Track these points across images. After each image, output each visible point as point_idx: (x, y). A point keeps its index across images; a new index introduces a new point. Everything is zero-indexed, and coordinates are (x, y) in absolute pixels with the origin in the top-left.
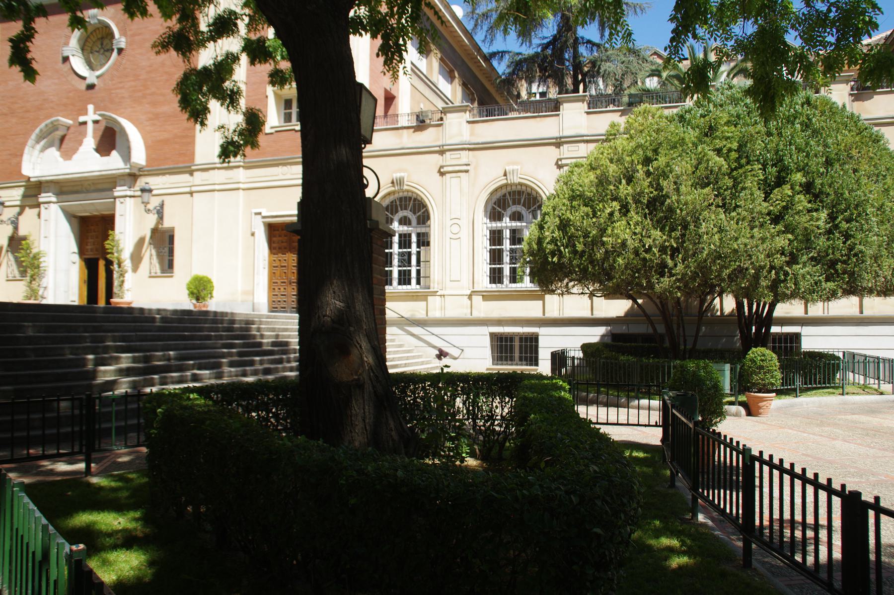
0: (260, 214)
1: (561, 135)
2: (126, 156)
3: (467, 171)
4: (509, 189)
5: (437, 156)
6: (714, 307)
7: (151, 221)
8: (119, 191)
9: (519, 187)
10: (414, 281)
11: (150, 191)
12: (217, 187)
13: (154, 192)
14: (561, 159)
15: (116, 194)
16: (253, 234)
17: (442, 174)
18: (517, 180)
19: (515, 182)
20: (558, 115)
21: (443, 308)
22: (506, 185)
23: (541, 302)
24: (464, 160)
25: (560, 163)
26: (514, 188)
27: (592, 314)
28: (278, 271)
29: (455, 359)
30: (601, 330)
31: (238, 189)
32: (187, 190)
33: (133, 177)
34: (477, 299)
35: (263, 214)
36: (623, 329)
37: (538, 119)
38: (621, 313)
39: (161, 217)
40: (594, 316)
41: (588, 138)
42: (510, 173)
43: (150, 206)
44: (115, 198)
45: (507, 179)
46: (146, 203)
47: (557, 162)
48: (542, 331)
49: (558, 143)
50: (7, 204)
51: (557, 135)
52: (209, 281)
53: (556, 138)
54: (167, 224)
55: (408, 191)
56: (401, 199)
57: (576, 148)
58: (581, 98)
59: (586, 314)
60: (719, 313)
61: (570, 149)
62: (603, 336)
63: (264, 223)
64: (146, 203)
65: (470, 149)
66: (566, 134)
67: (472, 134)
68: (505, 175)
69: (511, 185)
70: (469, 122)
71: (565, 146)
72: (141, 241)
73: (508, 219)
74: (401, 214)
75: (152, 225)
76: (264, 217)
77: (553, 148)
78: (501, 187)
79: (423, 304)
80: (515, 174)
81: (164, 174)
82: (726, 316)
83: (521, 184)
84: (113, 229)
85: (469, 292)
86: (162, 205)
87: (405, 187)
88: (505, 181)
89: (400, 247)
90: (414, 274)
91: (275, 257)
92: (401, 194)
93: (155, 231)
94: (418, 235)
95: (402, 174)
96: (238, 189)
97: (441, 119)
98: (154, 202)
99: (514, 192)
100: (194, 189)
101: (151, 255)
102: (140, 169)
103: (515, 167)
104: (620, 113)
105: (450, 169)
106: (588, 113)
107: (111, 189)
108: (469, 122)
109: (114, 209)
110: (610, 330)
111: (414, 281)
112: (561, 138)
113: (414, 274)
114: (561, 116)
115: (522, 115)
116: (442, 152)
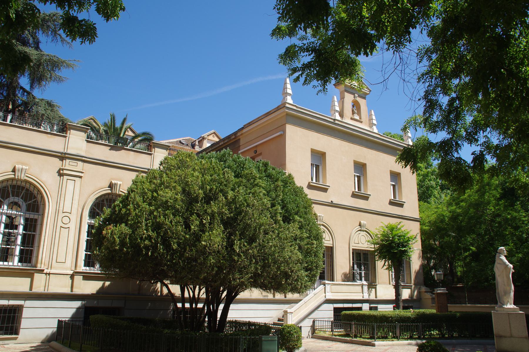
1: (66, 151)
4: (15, 182)
6: (157, 289)
9: (23, 184)
14: (63, 170)
18: (23, 177)
19: (22, 178)
20: (65, 137)
22: (12, 179)
23: (29, 280)
25: (61, 172)
26: (19, 183)
27: (72, 291)
30: (78, 304)
36: (95, 303)
37: (49, 135)
38: (94, 291)
40: (73, 293)
41: (86, 159)
42: (19, 171)
45: (15, 175)
47: (60, 169)
48: (28, 303)
49: (62, 157)
51: (62, 151)
53: (62, 153)
57: (76, 164)
58: (85, 130)
59: (67, 290)
60: (159, 294)
61: (71, 163)
62: (78, 309)
66: (69, 152)
68: (14, 170)
69: (17, 180)
71: (68, 161)
73: (6, 207)
77: (57, 160)
78: (7, 180)
80: (23, 173)
82: (164, 296)
83: (26, 182)
88: (13, 176)
99: (19, 187)
103: (24, 167)
104: (110, 148)
106: (88, 142)
110: (84, 304)
112: (65, 154)
114: (67, 138)
115: (35, 128)
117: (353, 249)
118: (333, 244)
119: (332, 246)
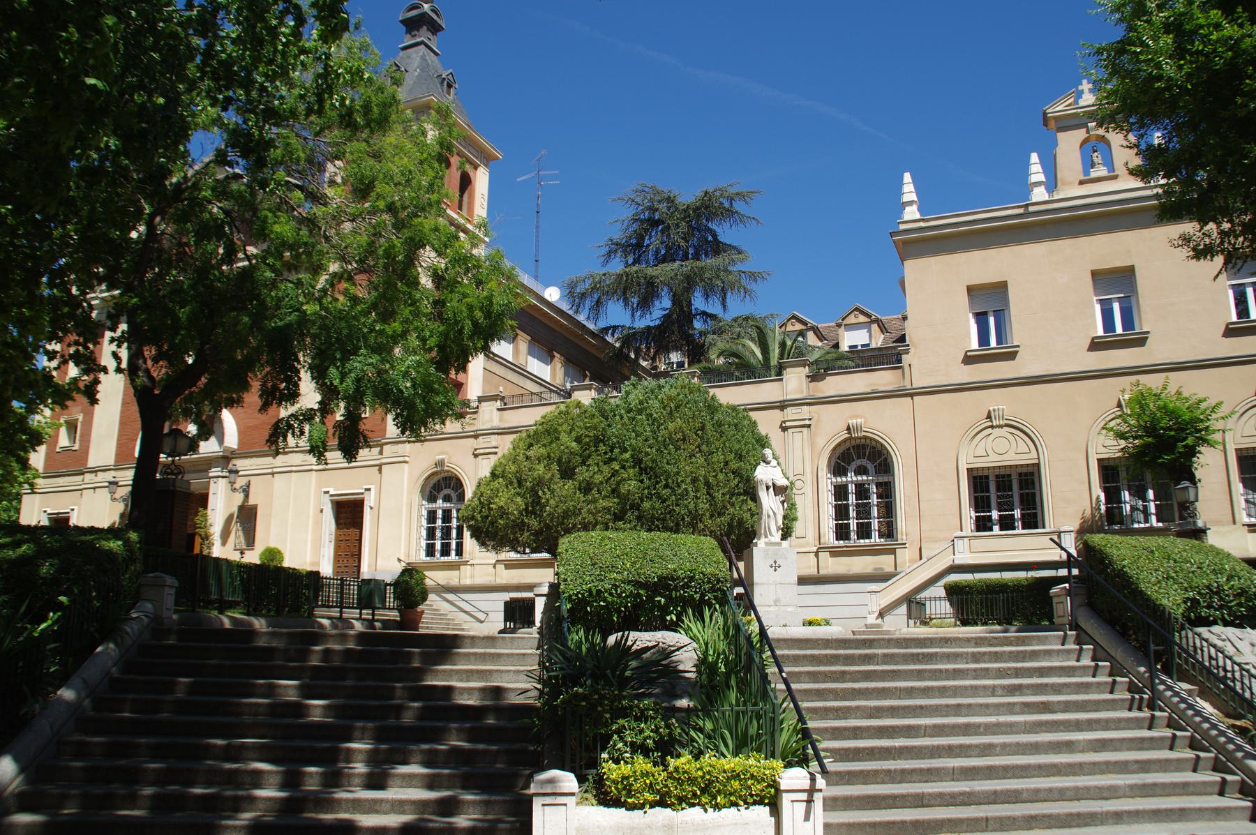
0: (328, 492)
2: (221, 441)
3: (495, 453)
5: (472, 440)
7: (239, 498)
8: (215, 472)
10: (453, 553)
11: (237, 472)
12: (294, 469)
13: (240, 473)
15: (211, 474)
16: (322, 511)
17: (476, 456)
21: (472, 576)
24: (494, 444)
28: (343, 545)
29: (482, 622)
31: (311, 470)
32: (270, 471)
33: (226, 459)
34: (501, 567)
35: (331, 493)
39: (247, 496)
43: (237, 486)
44: (210, 478)
46: (232, 483)
50: (120, 483)
52: (279, 552)
54: (252, 502)
55: (448, 471)
56: (446, 479)
63: (332, 501)
64: (232, 483)
65: (498, 434)
67: (501, 420)
70: (498, 410)
72: (230, 518)
74: (446, 491)
75: (240, 503)
76: (332, 496)
79: (456, 572)
81: (251, 457)
84: (206, 507)
85: (494, 562)
86: (248, 485)
87: (446, 468)
89: (443, 522)
90: (453, 546)
91: (341, 532)
92: (443, 475)
93: (241, 508)
94: (444, 511)
95: (441, 457)
96: (311, 470)
97: (477, 407)
98: (241, 482)
100: (275, 470)
101: (237, 530)
102: (233, 452)
105: (482, 451)
107: (207, 471)
108: (498, 410)
109: (208, 489)
111: (453, 553)
113: (453, 546)
116: (476, 437)
117: (1099, 460)
118: (1039, 458)
119: (1036, 461)
